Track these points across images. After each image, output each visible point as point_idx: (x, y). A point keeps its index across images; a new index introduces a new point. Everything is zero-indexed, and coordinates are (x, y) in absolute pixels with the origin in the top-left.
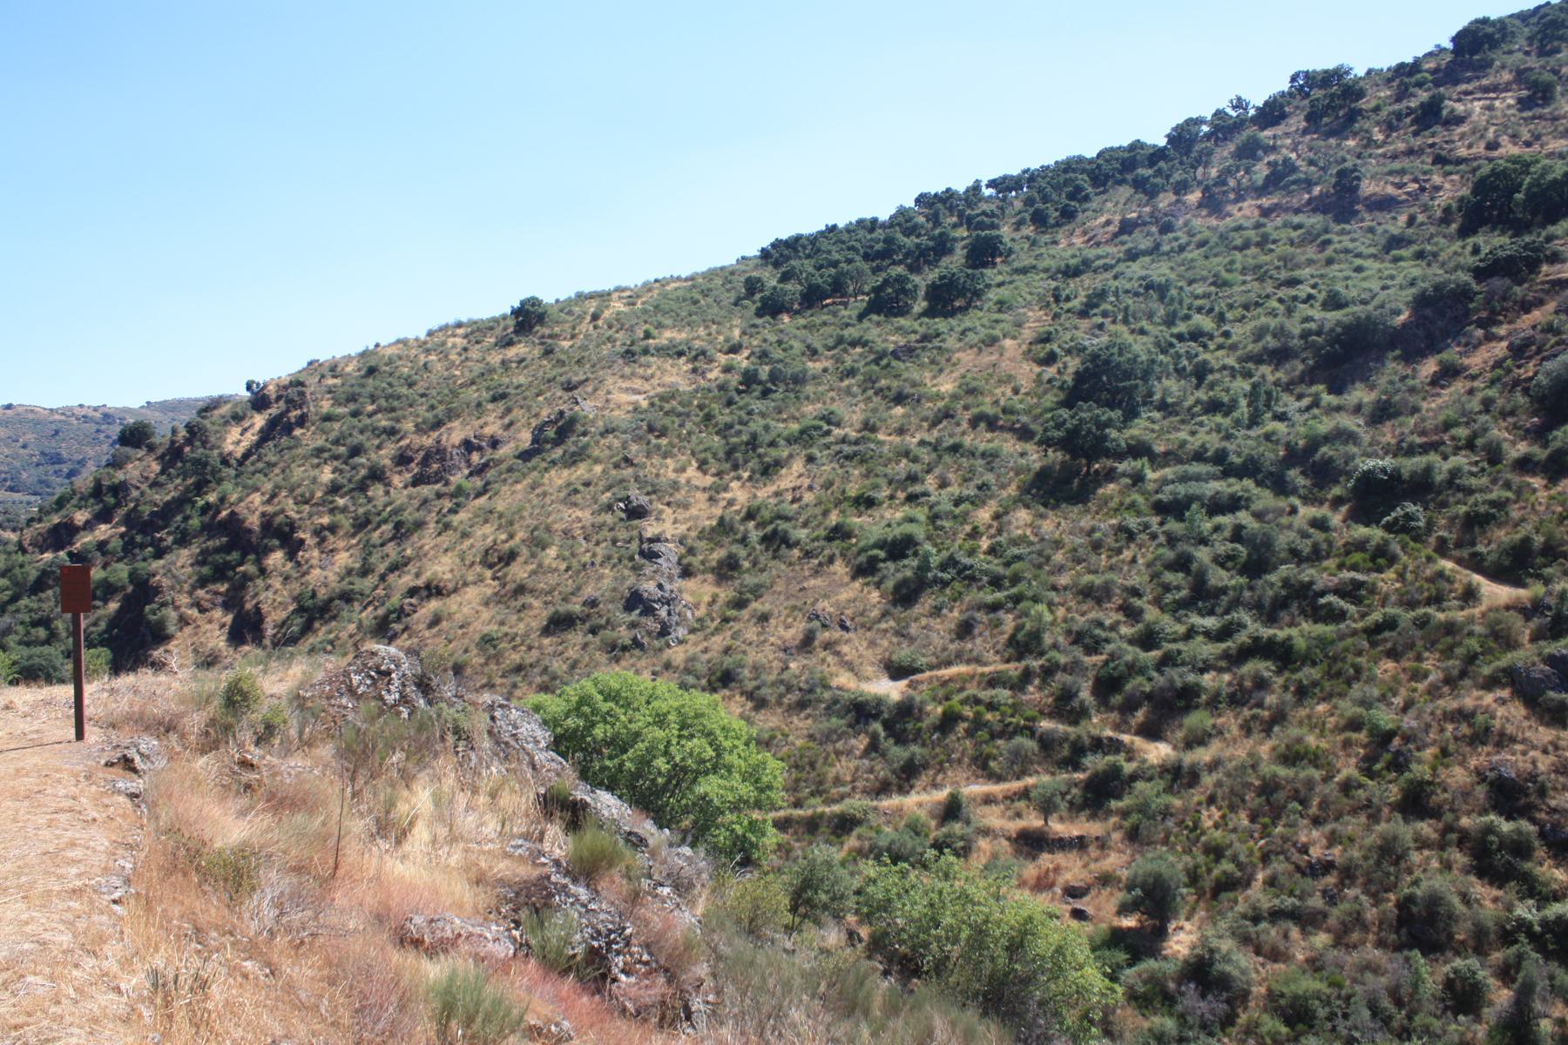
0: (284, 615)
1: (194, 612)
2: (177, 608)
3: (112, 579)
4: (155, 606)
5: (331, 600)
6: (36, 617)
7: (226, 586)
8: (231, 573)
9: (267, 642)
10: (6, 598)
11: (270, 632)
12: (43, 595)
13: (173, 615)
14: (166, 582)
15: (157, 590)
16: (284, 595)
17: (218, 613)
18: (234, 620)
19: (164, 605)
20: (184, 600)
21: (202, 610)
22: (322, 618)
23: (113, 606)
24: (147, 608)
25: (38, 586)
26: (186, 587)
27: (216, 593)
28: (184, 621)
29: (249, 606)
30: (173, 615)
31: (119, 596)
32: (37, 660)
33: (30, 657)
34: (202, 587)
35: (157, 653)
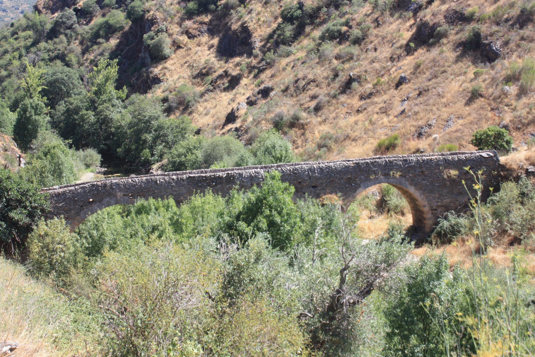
0: (269, 31)
1: (184, 39)
2: (170, 35)
3: (111, 22)
4: (152, 33)
5: (319, 9)
6: (52, 55)
7: (210, 17)
8: (212, 7)
9: (256, 51)
10: (29, 42)
11: (258, 44)
12: (56, 40)
13: (168, 41)
14: (159, 15)
15: (153, 22)
16: (266, 16)
17: (205, 38)
18: (220, 42)
19: (158, 31)
20: (175, 29)
21: (191, 37)
22: (312, 23)
23: (113, 42)
24: (145, 36)
25: (53, 34)
26: (176, 19)
27: (202, 23)
28: (177, 46)
29: (235, 27)
30: (168, 41)
31: (119, 34)
32: (60, 75)
33: (54, 74)
34: (189, 18)
35: (156, 70)
